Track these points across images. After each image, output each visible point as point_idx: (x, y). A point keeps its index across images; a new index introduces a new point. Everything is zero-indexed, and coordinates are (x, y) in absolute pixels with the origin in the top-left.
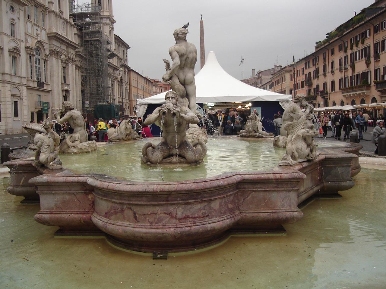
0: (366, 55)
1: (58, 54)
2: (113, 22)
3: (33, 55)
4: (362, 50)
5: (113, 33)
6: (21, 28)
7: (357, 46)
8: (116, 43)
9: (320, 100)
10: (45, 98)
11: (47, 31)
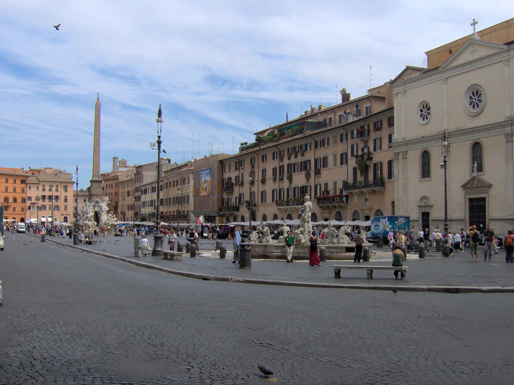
0: (306, 169)
4: (301, 163)
7: (296, 157)
9: (244, 211)
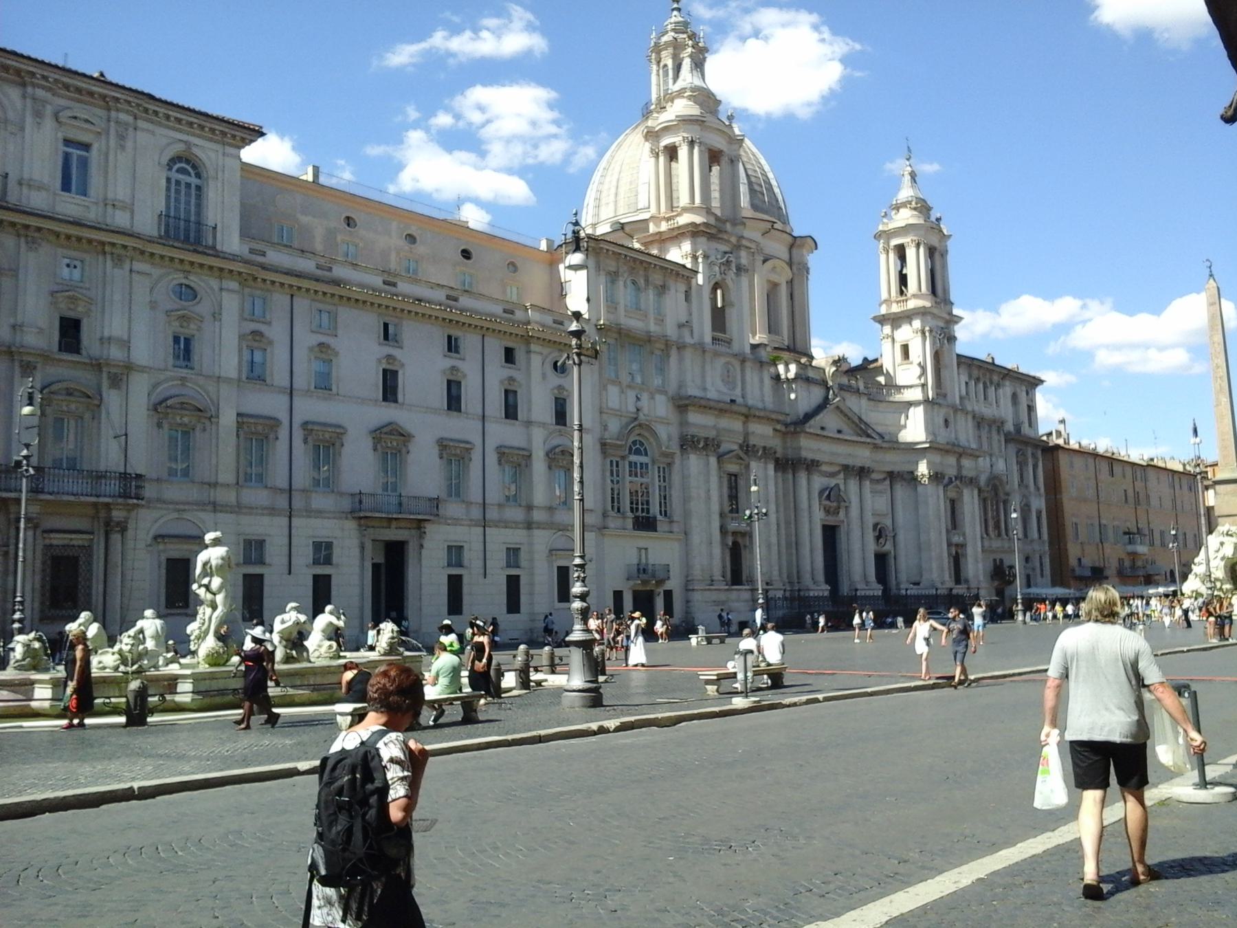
1: (709, 445)
3: (623, 458)
5: (951, 350)
8: (970, 377)
11: (670, 394)
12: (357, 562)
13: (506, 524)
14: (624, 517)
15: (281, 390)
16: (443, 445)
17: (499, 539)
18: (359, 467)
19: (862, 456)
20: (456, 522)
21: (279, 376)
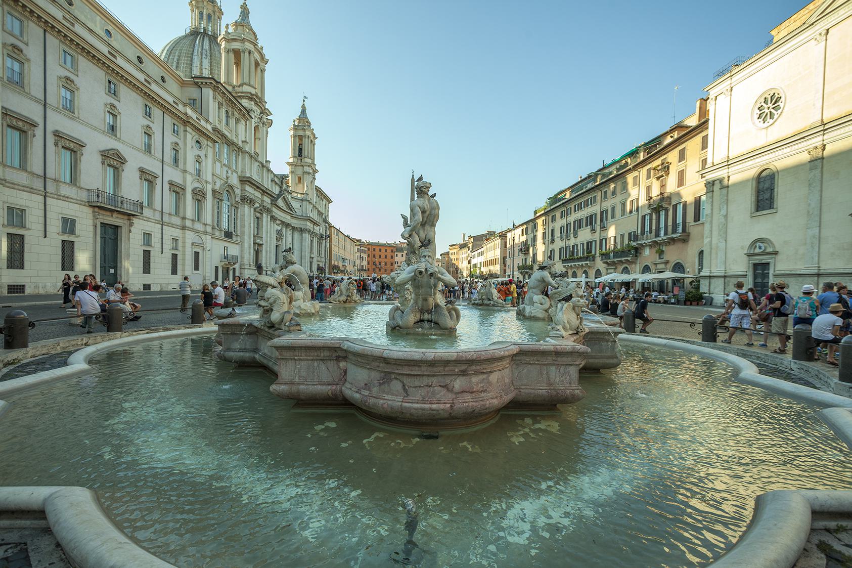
1: (251, 202)
2: (315, 171)
6: (208, 166)
10: (233, 250)
11: (239, 174)
12: (91, 235)
13: (172, 226)
14: (221, 230)
15: (37, 101)
16: (142, 171)
17: (170, 233)
18: (93, 174)
19: (287, 218)
20: (148, 220)
21: (36, 90)
